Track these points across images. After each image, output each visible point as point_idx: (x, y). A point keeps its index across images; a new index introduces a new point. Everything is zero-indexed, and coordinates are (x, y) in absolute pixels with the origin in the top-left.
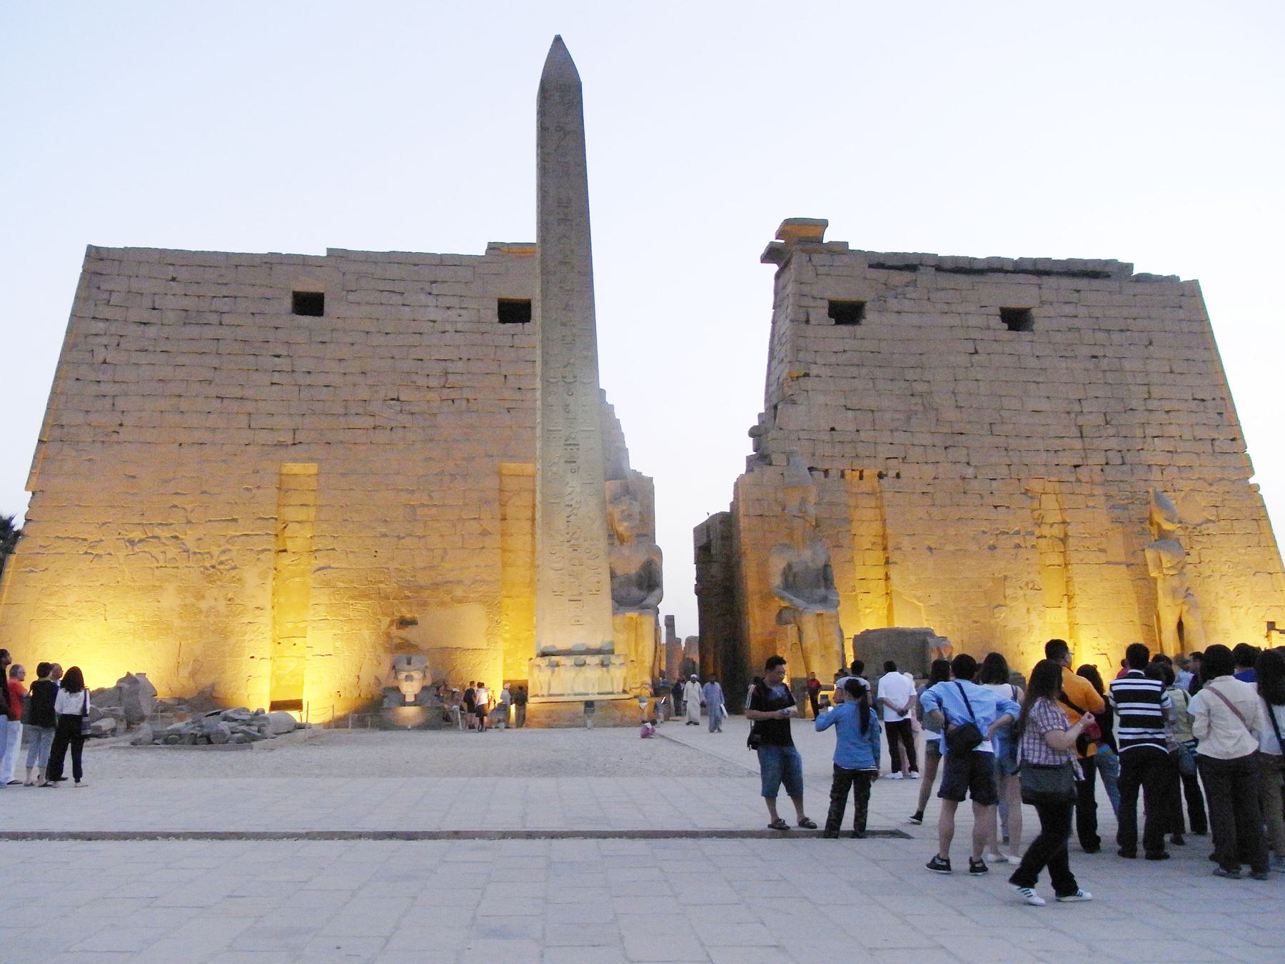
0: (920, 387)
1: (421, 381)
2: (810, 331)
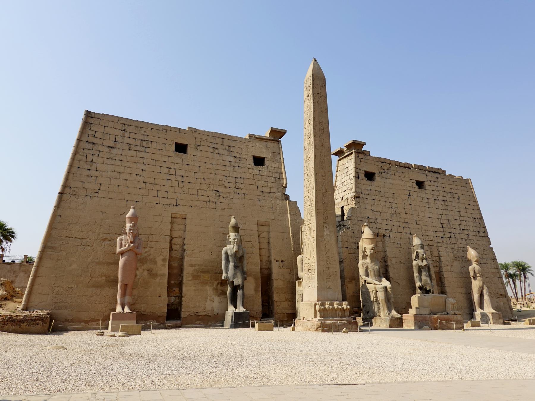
0: (394, 205)
1: (227, 185)
2: (359, 181)
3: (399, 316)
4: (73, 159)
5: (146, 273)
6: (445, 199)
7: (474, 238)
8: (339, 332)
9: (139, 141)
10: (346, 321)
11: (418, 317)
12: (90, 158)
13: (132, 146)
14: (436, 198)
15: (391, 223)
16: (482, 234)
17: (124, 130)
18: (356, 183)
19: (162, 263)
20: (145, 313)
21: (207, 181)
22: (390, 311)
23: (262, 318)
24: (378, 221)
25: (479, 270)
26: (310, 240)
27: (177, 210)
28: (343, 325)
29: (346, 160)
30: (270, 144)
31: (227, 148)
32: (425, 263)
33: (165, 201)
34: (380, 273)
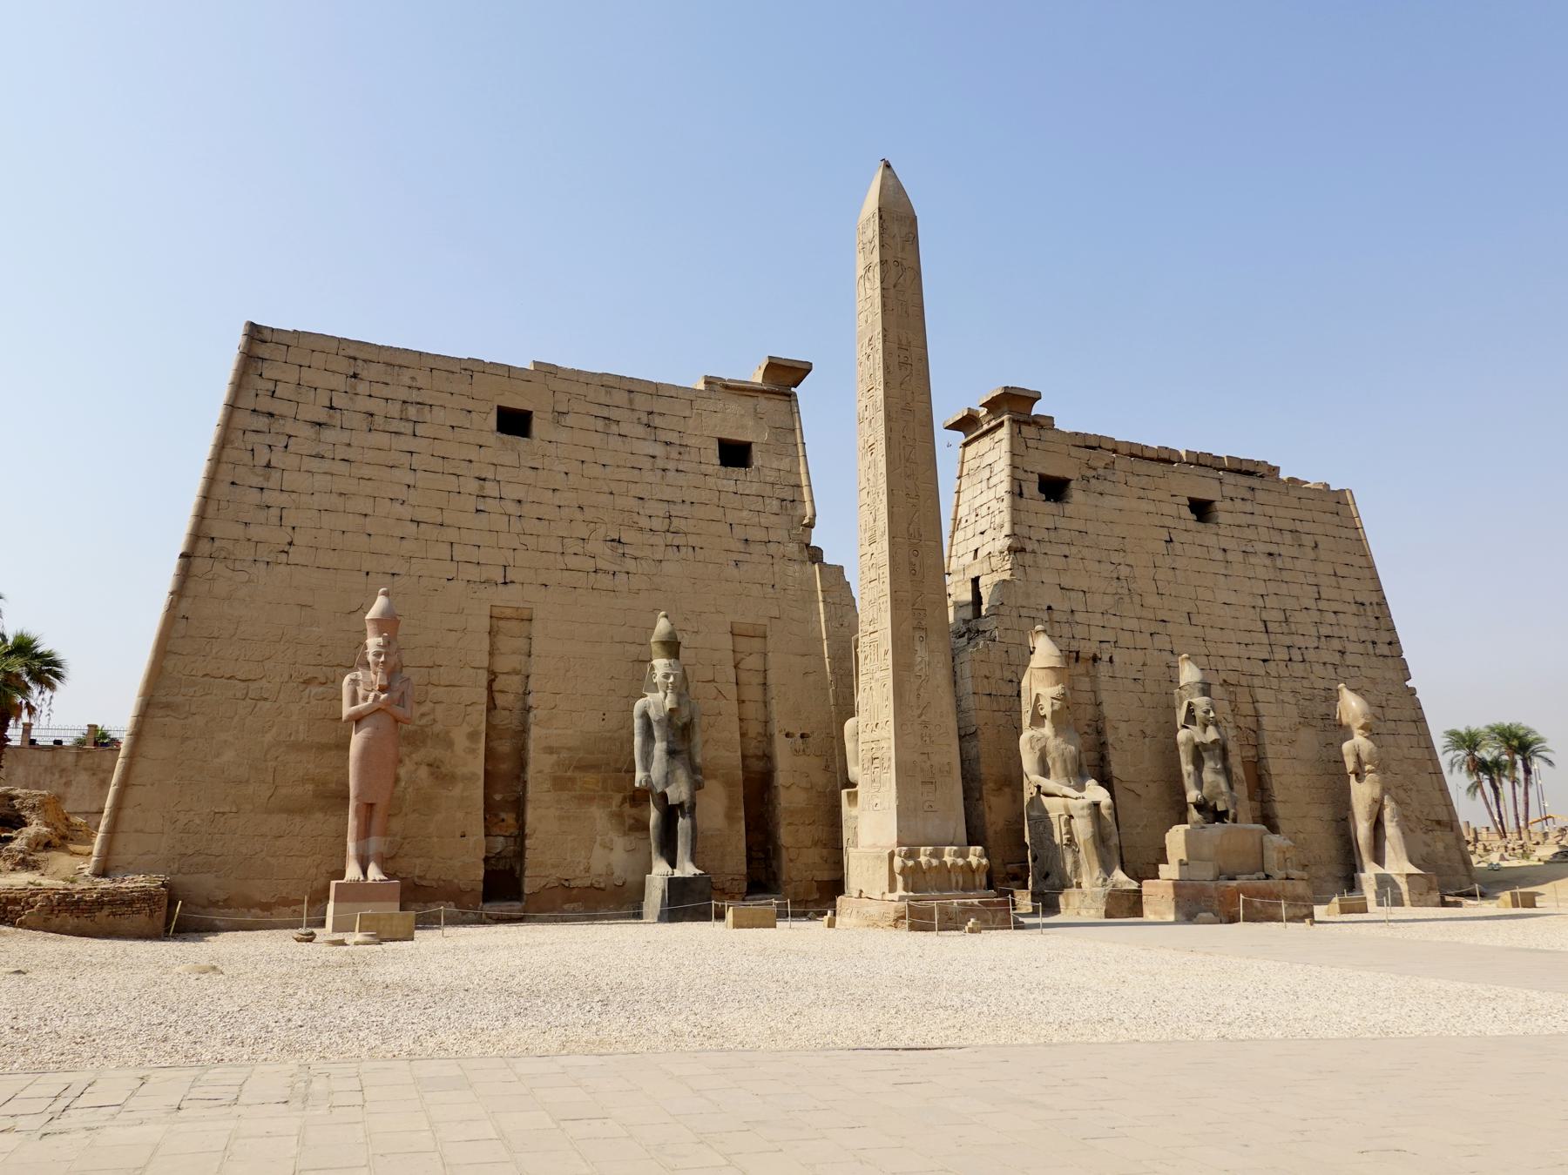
0: (1124, 571)
1: (644, 522)
2: (1023, 503)
3: (1134, 885)
4: (217, 460)
5: (423, 772)
6: (1273, 549)
7: (1359, 660)
8: (957, 929)
9: (398, 406)
10: (976, 901)
11: (1184, 887)
13: (379, 420)
14: (1249, 549)
15: (1115, 622)
16: (1385, 650)
17: (355, 376)
18: (1014, 509)
19: (467, 743)
20: (424, 883)
21: (590, 514)
22: (1107, 870)
23: (748, 893)
24: (1079, 617)
25: (1370, 754)
26: (877, 676)
28: (968, 911)
29: (986, 441)
30: (764, 404)
31: (645, 419)
32: (1212, 734)
33: (472, 573)
34: (1080, 765)
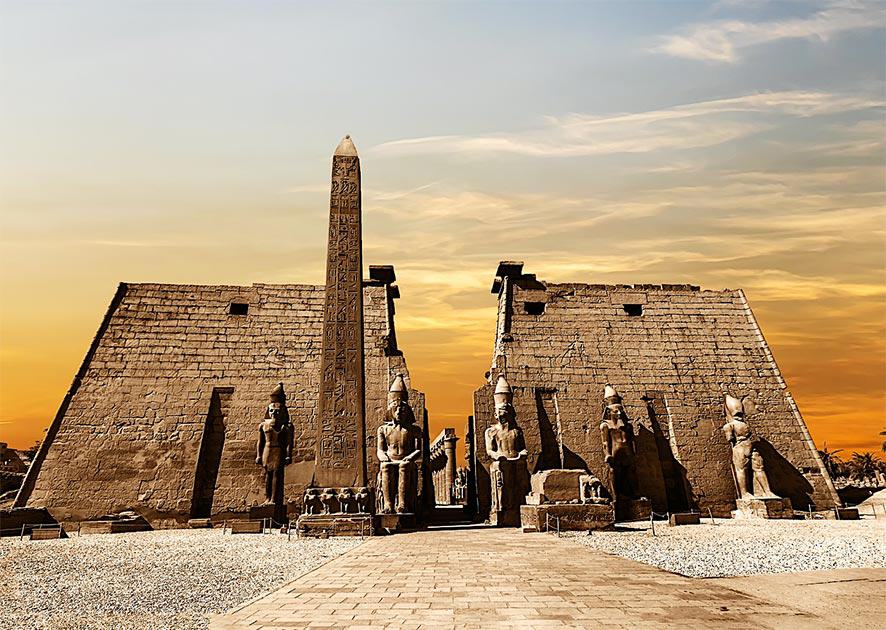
12: (119, 334)
21: (269, 345)
27: (225, 383)
